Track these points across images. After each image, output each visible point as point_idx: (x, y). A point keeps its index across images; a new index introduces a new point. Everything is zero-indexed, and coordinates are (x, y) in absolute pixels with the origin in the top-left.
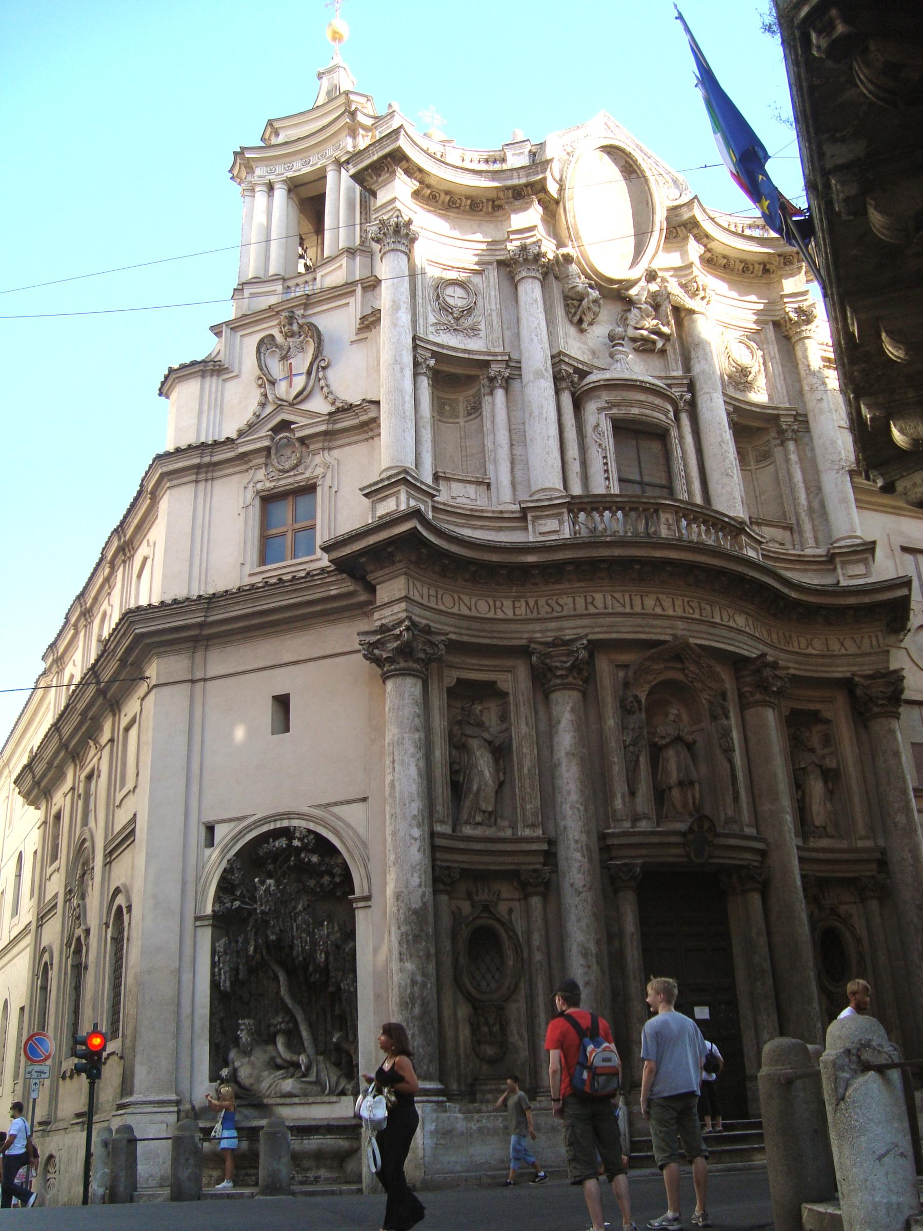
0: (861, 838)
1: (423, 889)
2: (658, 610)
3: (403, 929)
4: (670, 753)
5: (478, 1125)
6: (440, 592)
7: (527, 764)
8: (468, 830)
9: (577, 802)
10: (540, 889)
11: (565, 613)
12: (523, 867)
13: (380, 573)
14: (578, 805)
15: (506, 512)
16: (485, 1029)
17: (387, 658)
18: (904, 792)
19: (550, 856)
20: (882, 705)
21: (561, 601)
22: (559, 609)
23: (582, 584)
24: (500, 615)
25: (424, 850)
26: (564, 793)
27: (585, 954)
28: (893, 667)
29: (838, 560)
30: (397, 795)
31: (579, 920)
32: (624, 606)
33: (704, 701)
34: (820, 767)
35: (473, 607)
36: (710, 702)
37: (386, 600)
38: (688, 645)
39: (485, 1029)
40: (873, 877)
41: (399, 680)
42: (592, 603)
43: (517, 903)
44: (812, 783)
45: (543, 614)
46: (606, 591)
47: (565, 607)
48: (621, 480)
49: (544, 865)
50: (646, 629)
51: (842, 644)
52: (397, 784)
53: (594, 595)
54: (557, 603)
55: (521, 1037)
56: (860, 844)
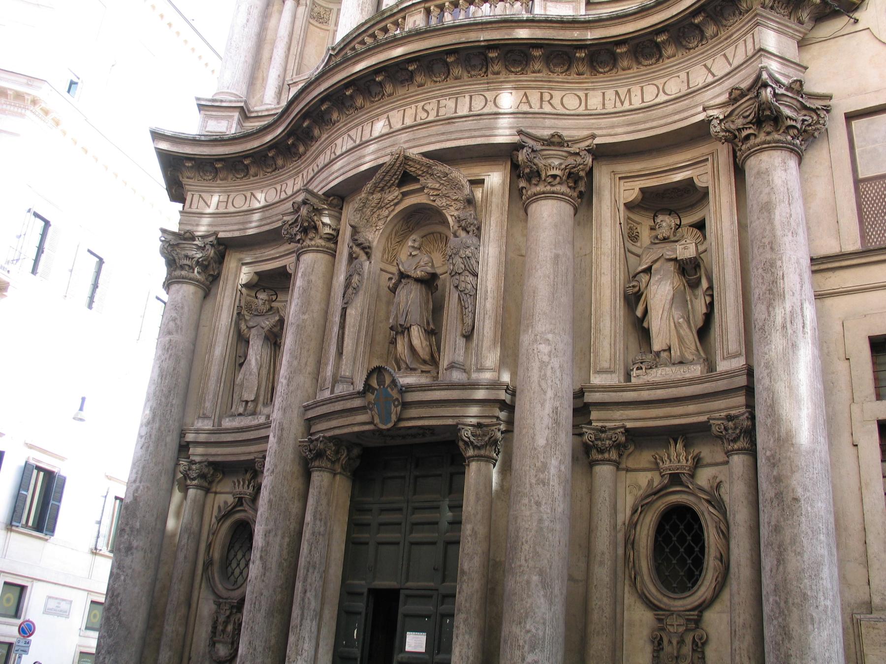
1: (137, 484)
8: (227, 423)
20: (747, 137)
25: (148, 447)
32: (355, 142)
33: (450, 219)
38: (406, 158)
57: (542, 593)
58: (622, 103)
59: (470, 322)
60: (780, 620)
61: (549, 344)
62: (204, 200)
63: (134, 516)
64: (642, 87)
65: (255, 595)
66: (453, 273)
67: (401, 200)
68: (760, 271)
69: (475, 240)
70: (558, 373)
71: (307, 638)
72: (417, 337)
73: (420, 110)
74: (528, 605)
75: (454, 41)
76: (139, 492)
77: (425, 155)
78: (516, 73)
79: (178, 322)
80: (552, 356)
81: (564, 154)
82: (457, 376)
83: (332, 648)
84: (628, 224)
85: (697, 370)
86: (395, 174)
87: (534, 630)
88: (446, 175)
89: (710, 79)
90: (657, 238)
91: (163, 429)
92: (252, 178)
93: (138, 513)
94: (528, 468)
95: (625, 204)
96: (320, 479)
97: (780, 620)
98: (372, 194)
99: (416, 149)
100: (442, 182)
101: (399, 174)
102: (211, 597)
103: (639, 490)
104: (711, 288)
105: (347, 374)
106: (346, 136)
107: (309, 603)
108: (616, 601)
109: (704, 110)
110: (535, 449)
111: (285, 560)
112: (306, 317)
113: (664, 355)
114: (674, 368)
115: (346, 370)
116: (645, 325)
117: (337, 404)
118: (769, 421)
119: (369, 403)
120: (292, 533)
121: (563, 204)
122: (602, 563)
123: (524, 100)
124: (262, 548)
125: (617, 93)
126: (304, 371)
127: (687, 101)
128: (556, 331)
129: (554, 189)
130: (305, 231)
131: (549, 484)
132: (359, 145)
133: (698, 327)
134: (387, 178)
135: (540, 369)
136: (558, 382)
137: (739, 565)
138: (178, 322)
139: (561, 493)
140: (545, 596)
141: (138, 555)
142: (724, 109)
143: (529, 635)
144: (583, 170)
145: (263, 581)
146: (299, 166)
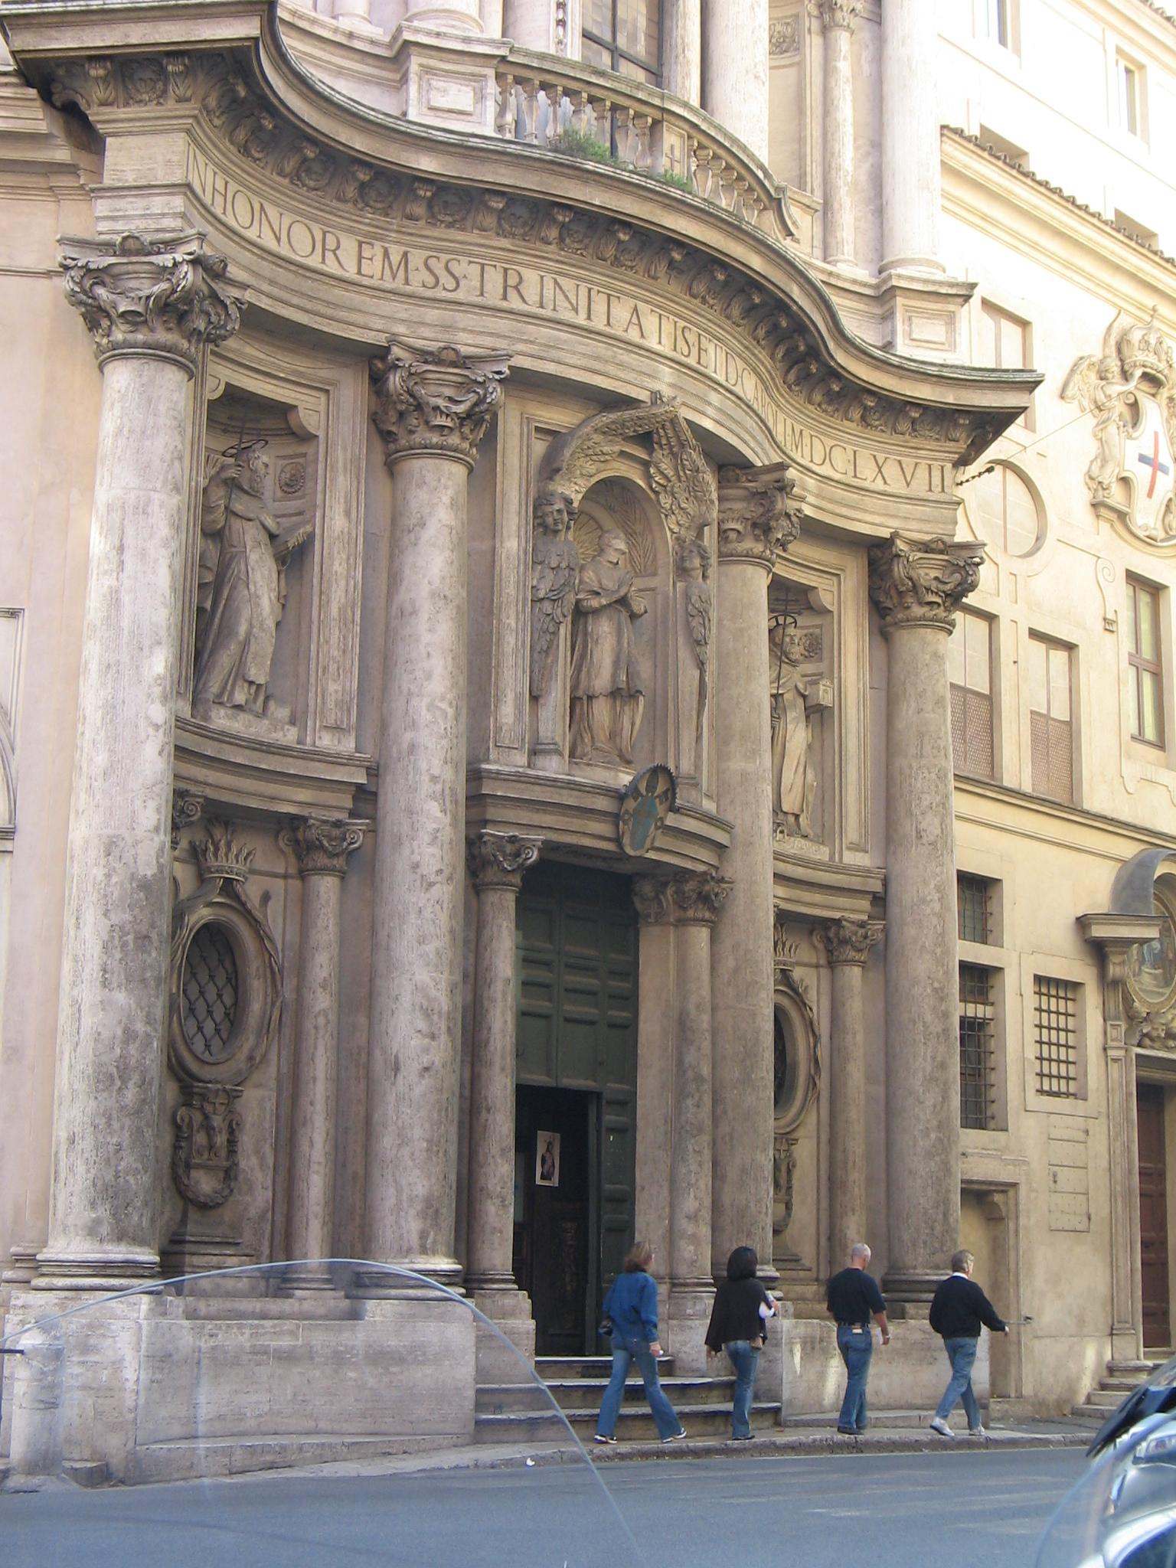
0: (855, 848)
2: (634, 335)
3: (117, 918)
4: (604, 629)
5: (212, 1343)
7: (338, 596)
9: (443, 699)
10: (339, 862)
11: (460, 295)
12: (315, 813)
13: (122, 113)
14: (444, 705)
15: (359, 38)
16: (200, 1138)
17: (123, 315)
18: (942, 776)
19: (366, 798)
20: (930, 603)
21: (455, 267)
22: (451, 285)
23: (505, 243)
24: (331, 267)
26: (419, 674)
27: (427, 1013)
28: (961, 536)
29: (900, 301)
30: (126, 623)
31: (422, 940)
34: (804, 697)
35: (284, 238)
36: (679, 540)
37: (130, 179)
38: (674, 421)
39: (200, 1138)
40: (862, 925)
41: (150, 369)
42: (516, 288)
43: (281, 882)
44: (790, 727)
45: (414, 288)
46: (549, 271)
47: (462, 283)
48: (586, 35)
49: (353, 814)
50: (611, 369)
51: (880, 471)
52: (126, 599)
53: (524, 272)
54: (447, 268)
55: (262, 1158)
56: (850, 858)
58: (797, 447)
60: (943, 1156)
65: (445, 1096)
68: (933, 776)
97: (943, 1156)
100: (681, 473)
118: (938, 951)
124: (449, 1013)
127: (855, 496)
146: (386, 230)
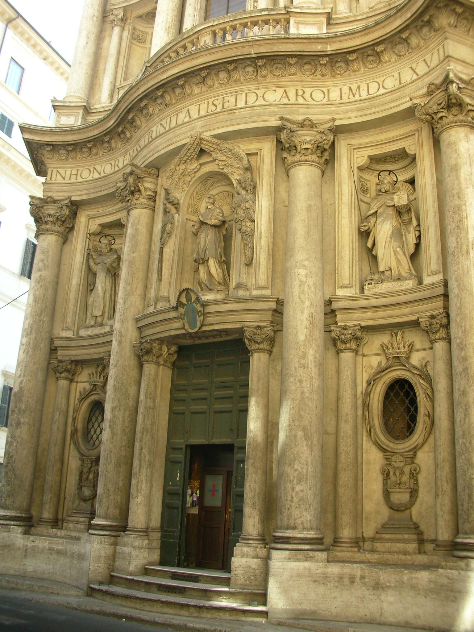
1: (22, 378)
5: (33, 544)
6: (81, 169)
8: (83, 333)
25: (28, 352)
32: (165, 128)
33: (234, 182)
50: (174, 140)
51: (414, 71)
57: (305, 443)
58: (354, 96)
59: (250, 254)
61: (306, 269)
62: (60, 174)
63: (21, 400)
64: (368, 84)
65: (107, 453)
66: (237, 221)
67: (199, 169)
69: (252, 196)
70: (313, 289)
71: (144, 481)
72: (214, 267)
73: (210, 104)
74: (296, 452)
75: (233, 55)
76: (23, 384)
77: (214, 136)
78: (278, 76)
79: (46, 262)
80: (308, 277)
81: (315, 133)
82: (241, 293)
83: (162, 487)
84: (360, 181)
85: (410, 284)
86: (194, 151)
87: (300, 469)
88: (230, 150)
89: (415, 77)
90: (380, 191)
91: (38, 338)
92: (94, 157)
93: (23, 399)
94: (293, 356)
95: (358, 167)
96: (149, 369)
98: (179, 165)
99: (208, 132)
100: (228, 155)
101: (197, 150)
102: (77, 455)
103: (372, 369)
104: (419, 225)
105: (165, 294)
106: (159, 125)
107: (145, 457)
108: (357, 447)
109: (411, 99)
110: (298, 343)
111: (127, 427)
112: (135, 255)
113: (387, 273)
114: (394, 283)
115: (164, 292)
116: (374, 253)
117: (158, 316)
119: (181, 314)
120: (131, 408)
121: (313, 168)
122: (347, 421)
123: (285, 95)
124: (110, 419)
125: (350, 88)
126: (135, 293)
128: (311, 259)
129: (307, 158)
130: (133, 193)
131: (308, 367)
132: (168, 131)
133: (411, 253)
134: (188, 154)
135: (300, 286)
136: (313, 295)
137: (440, 419)
138: (46, 262)
139: (317, 373)
140: (307, 445)
141: (25, 428)
142: (425, 98)
143: (297, 472)
144: (327, 144)
145: (112, 443)
